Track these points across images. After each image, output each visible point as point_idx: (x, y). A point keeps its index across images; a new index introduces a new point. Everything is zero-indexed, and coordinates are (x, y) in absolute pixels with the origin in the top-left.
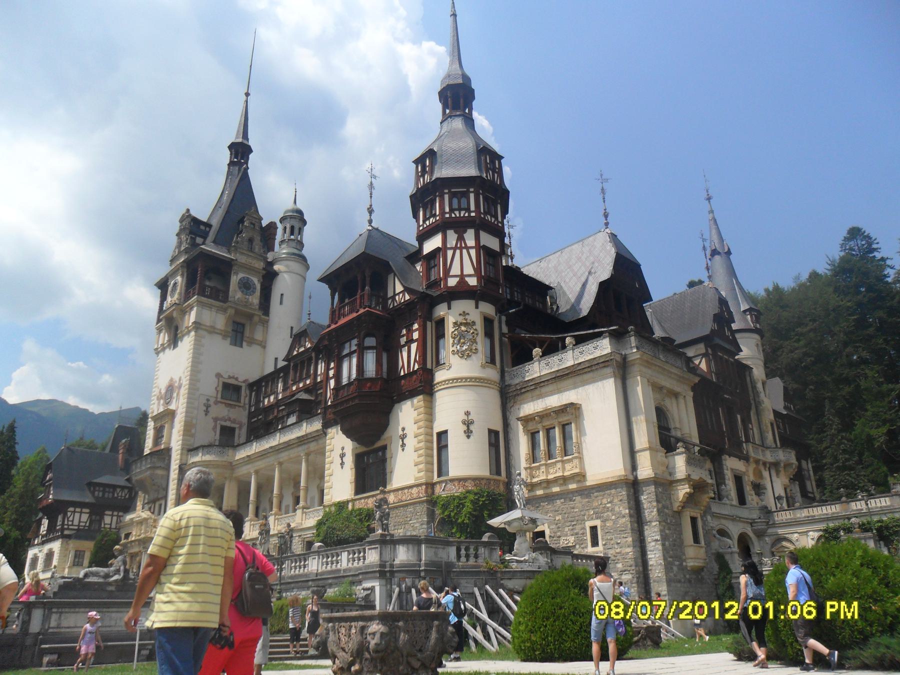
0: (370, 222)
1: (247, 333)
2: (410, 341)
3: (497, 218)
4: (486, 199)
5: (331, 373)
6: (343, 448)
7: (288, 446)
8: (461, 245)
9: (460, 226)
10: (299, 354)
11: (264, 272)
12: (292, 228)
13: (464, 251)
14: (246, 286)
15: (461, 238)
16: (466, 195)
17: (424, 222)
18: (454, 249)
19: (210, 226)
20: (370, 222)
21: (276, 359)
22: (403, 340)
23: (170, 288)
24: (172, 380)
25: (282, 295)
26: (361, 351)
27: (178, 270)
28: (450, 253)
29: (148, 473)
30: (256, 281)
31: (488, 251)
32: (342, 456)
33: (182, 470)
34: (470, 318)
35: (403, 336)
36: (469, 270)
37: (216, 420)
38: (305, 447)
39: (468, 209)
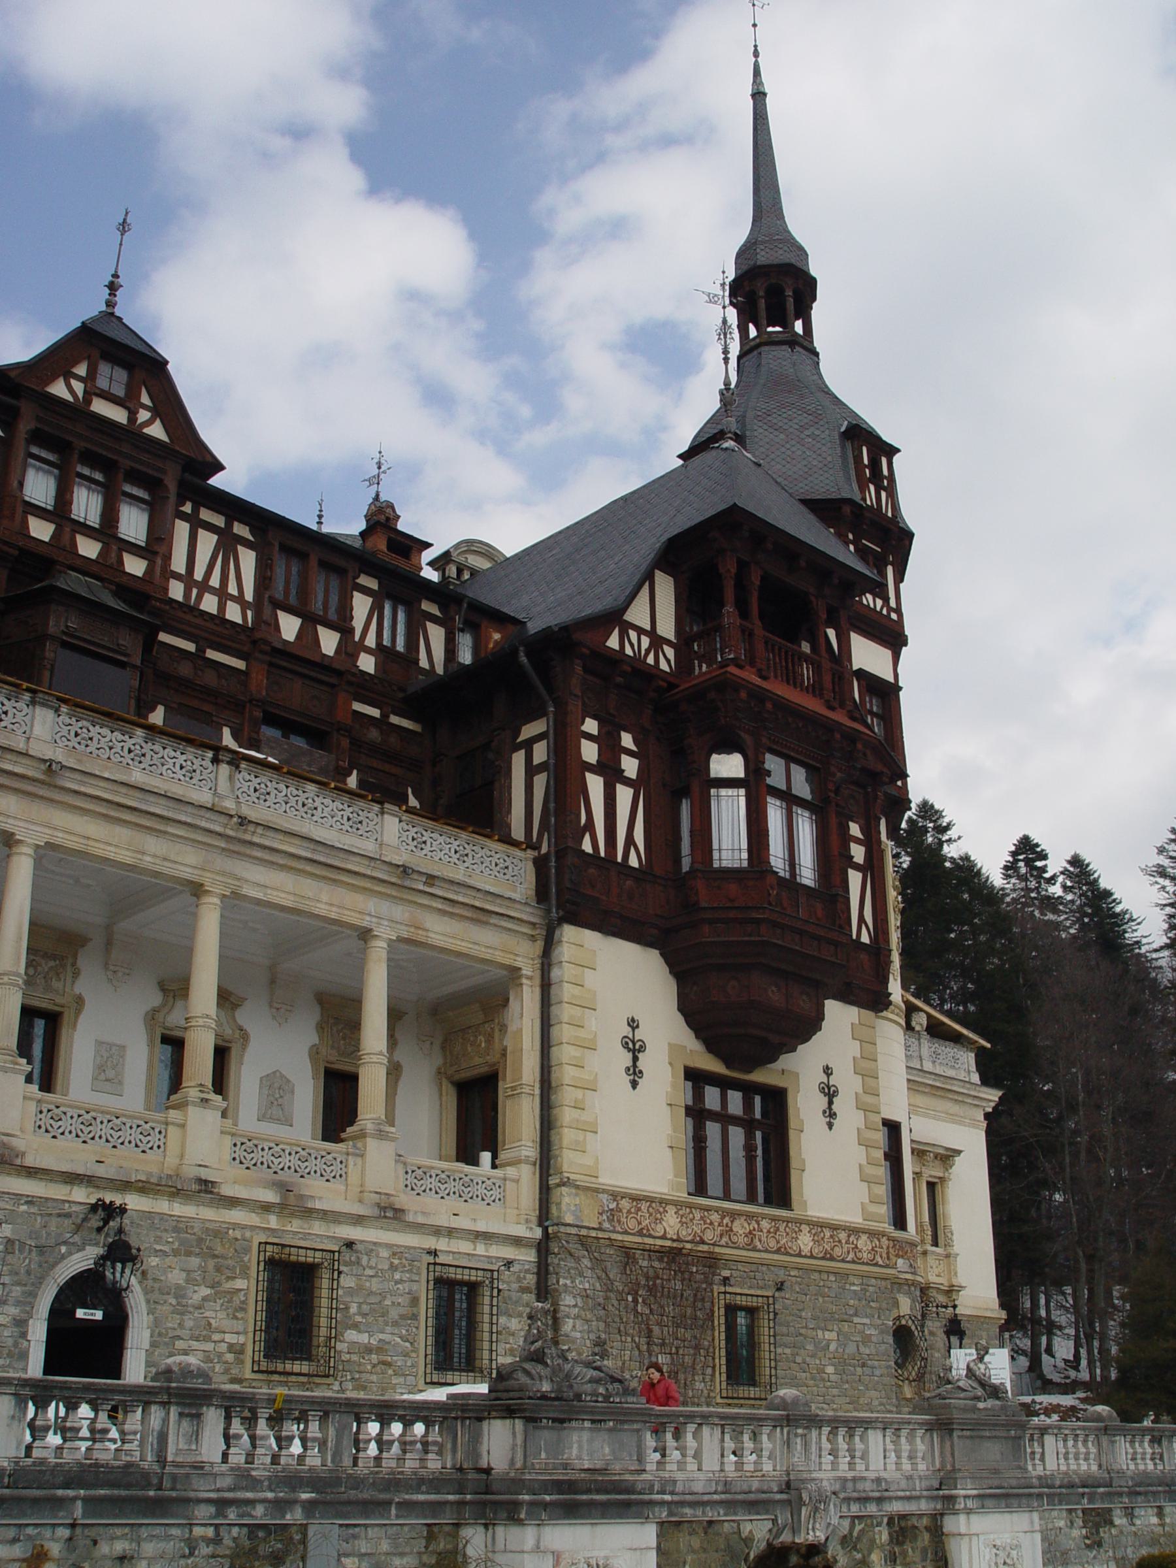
6: (633, 1024)
7: (326, 864)
10: (78, 412)
32: (635, 1048)
38: (399, 912)
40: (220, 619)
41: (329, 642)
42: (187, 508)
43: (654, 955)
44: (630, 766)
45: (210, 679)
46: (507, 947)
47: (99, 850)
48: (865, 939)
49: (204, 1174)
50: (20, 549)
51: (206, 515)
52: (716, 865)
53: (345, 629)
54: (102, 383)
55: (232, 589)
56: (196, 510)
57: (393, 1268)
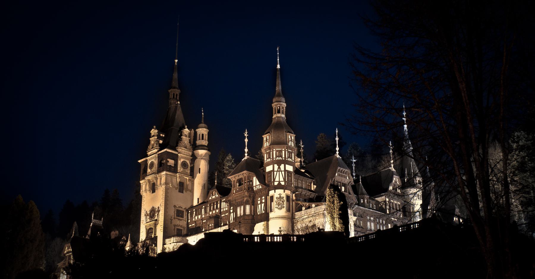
2: (261, 203)
3: (292, 158)
4: (289, 152)
5: (231, 211)
8: (279, 170)
9: (279, 163)
10: (213, 200)
11: (191, 158)
15: (279, 168)
18: (277, 171)
22: (259, 202)
24: (153, 207)
28: (275, 173)
30: (188, 162)
31: (289, 172)
34: (282, 196)
36: (282, 179)
39: (281, 156)
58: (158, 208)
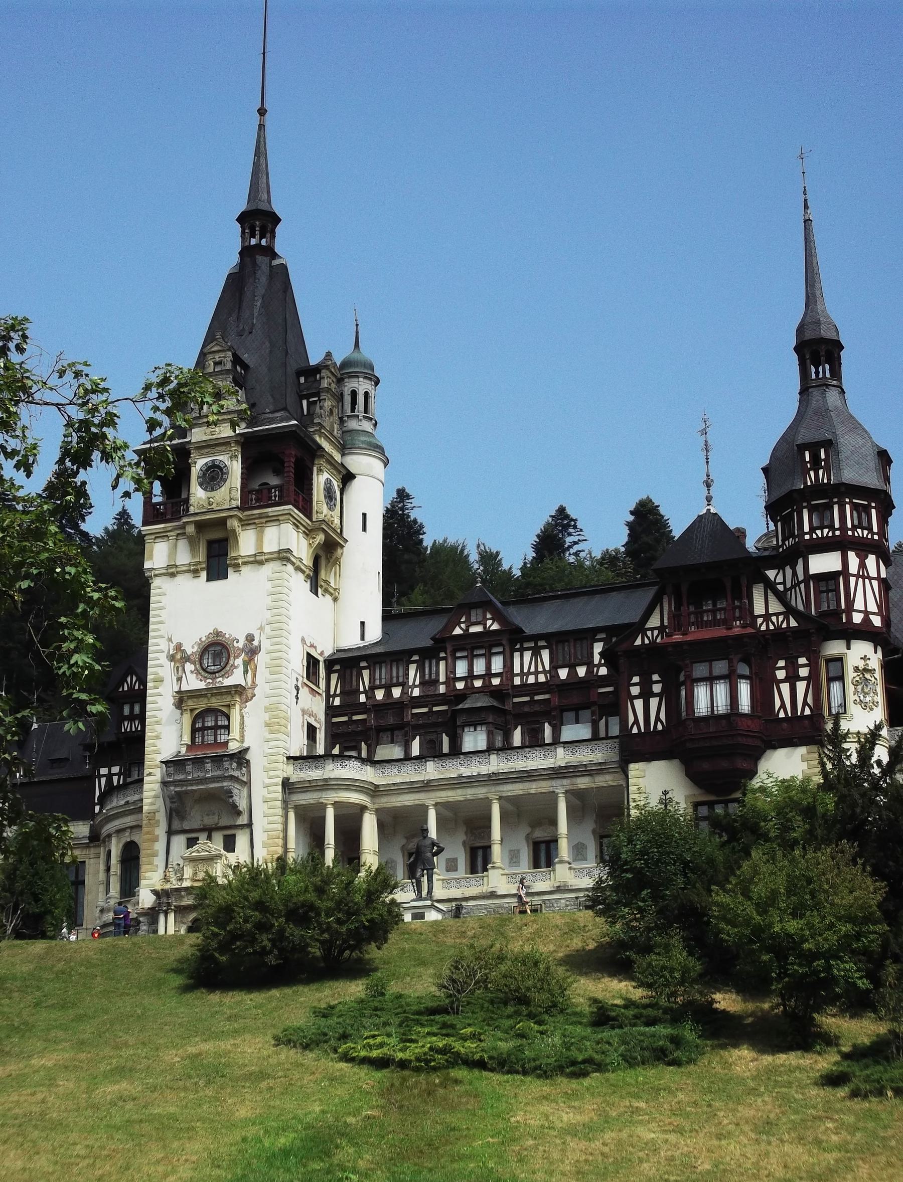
0: (709, 499)
1: (323, 575)
2: (792, 678)
5: (635, 691)
8: (863, 575)
9: (863, 548)
10: (466, 635)
12: (366, 395)
13: (867, 581)
14: (329, 495)
15: (862, 565)
16: (867, 509)
17: (812, 529)
18: (857, 576)
19: (245, 367)
20: (709, 499)
21: (363, 623)
22: (781, 674)
23: (195, 471)
25: (364, 515)
26: (732, 679)
27: (229, 443)
28: (852, 580)
29: (225, 784)
33: (287, 785)
35: (780, 668)
36: (872, 607)
37: (304, 712)
38: (565, 782)
39: (870, 529)
40: (537, 683)
41: (581, 671)
42: (518, 646)
43: (676, 762)
44: (657, 688)
45: (537, 708)
46: (605, 780)
47: (452, 799)
48: (807, 712)
49: (494, 889)
50: (454, 696)
51: (526, 645)
52: (696, 715)
53: (589, 663)
54: (473, 619)
55: (540, 669)
56: (522, 645)
57: (567, 906)
58: (250, 638)
